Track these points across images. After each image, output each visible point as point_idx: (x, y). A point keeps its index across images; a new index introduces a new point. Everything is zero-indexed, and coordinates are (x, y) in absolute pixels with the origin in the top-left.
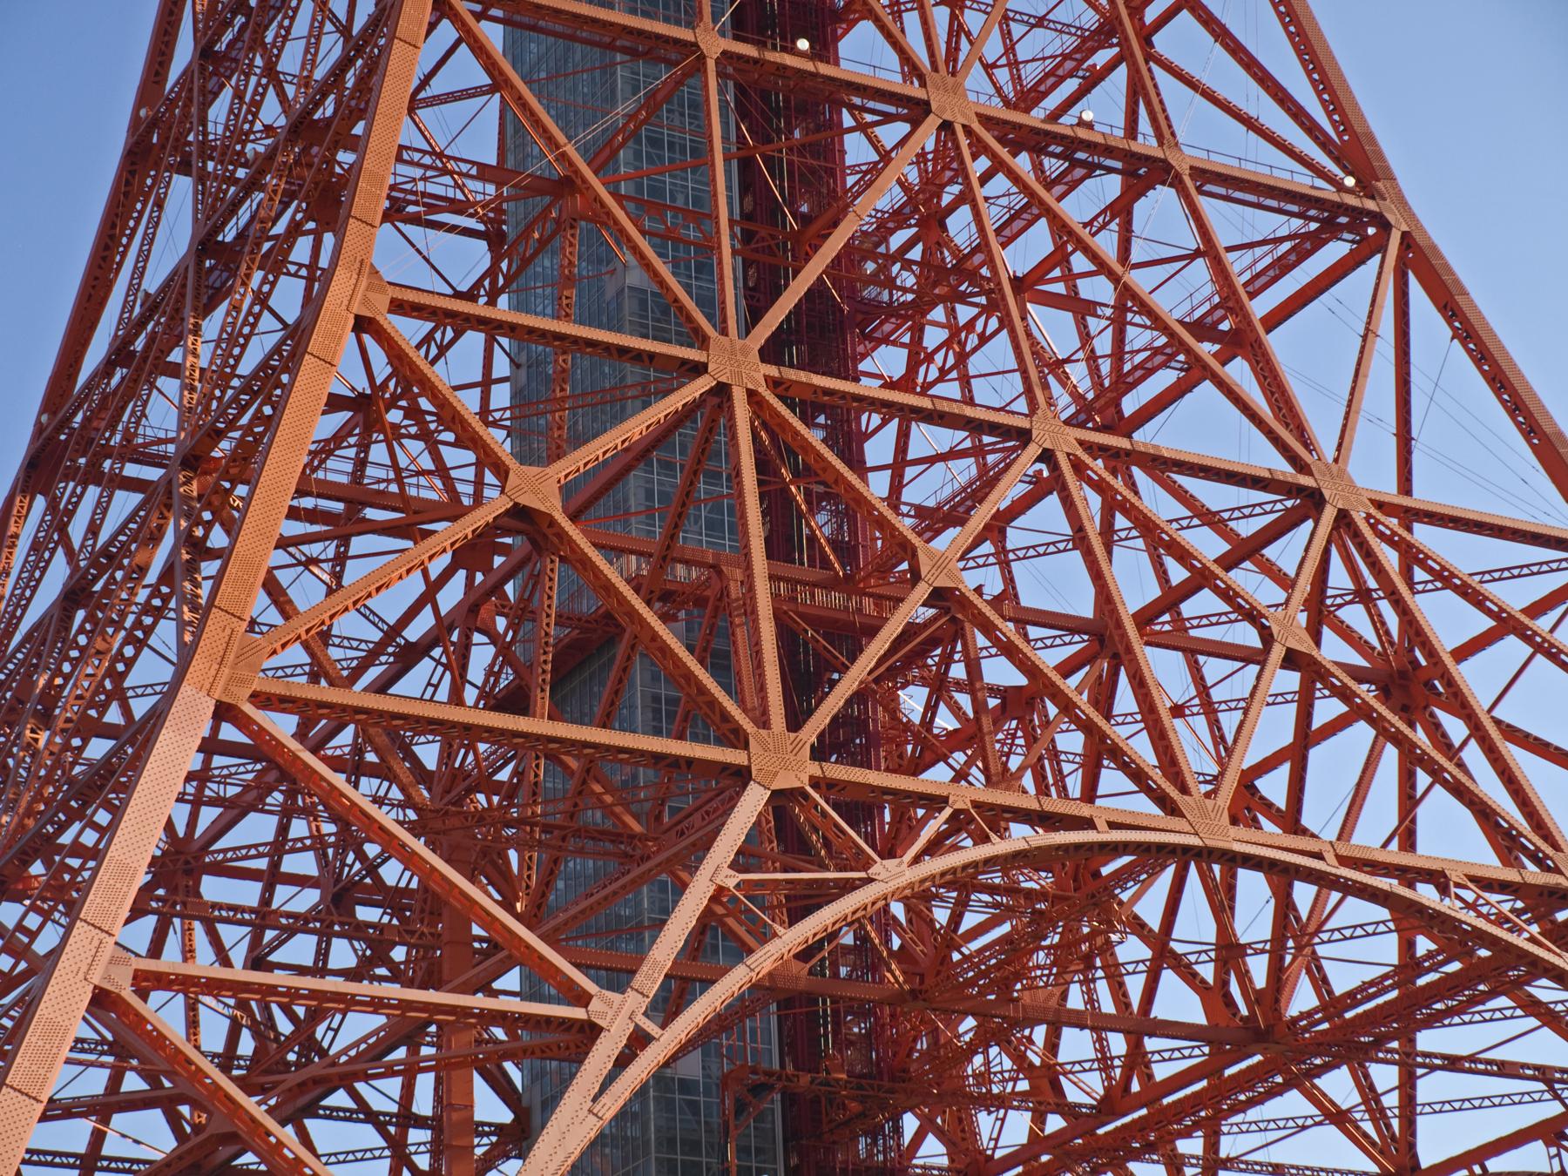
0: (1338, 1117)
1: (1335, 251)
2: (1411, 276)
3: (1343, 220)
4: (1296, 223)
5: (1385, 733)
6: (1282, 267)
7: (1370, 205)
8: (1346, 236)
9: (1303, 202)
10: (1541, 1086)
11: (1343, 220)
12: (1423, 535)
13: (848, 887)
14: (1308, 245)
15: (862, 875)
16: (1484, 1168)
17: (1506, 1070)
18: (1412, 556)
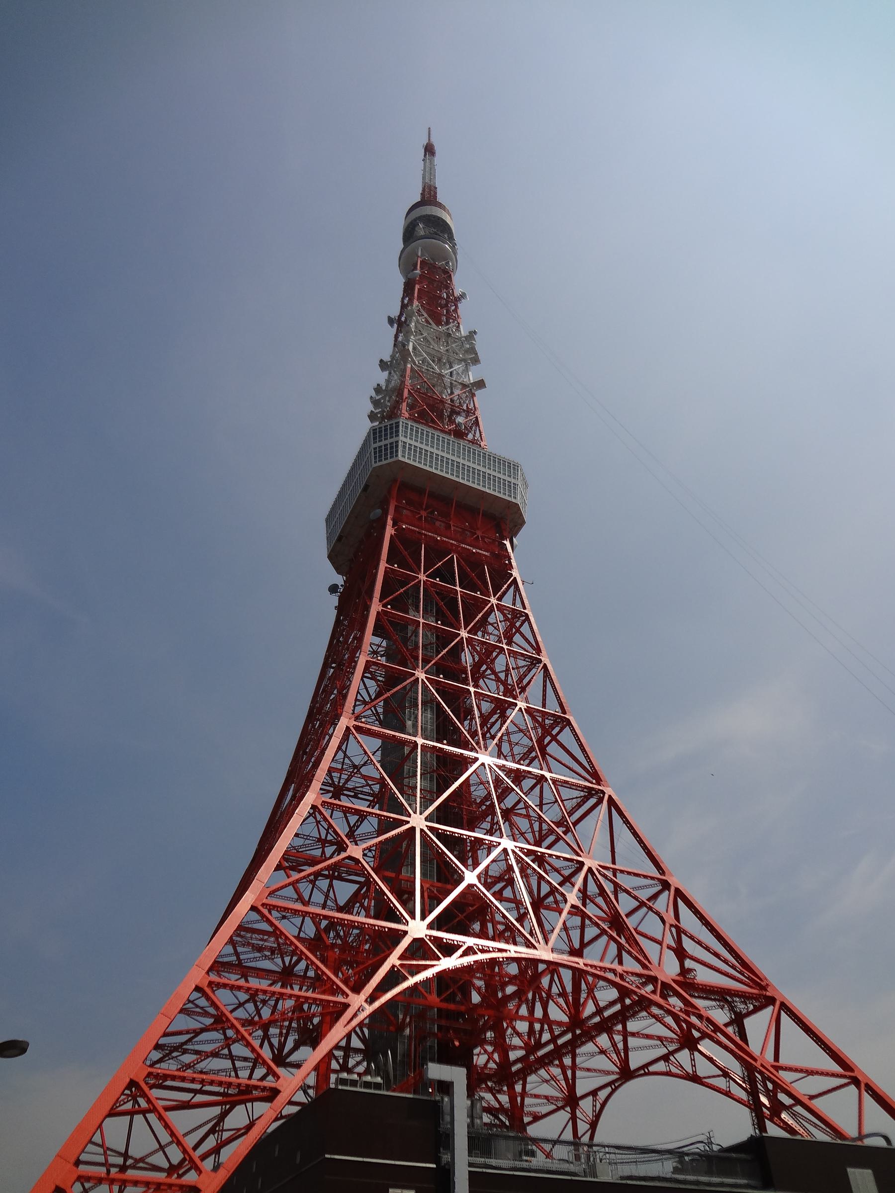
0: (602, 1052)
1: (593, 801)
3: (594, 792)
4: (582, 794)
5: (611, 938)
6: (579, 806)
8: (595, 797)
10: (659, 1042)
11: (594, 792)
12: (621, 879)
14: (585, 800)
16: (648, 1070)
17: (648, 1037)
18: (617, 886)
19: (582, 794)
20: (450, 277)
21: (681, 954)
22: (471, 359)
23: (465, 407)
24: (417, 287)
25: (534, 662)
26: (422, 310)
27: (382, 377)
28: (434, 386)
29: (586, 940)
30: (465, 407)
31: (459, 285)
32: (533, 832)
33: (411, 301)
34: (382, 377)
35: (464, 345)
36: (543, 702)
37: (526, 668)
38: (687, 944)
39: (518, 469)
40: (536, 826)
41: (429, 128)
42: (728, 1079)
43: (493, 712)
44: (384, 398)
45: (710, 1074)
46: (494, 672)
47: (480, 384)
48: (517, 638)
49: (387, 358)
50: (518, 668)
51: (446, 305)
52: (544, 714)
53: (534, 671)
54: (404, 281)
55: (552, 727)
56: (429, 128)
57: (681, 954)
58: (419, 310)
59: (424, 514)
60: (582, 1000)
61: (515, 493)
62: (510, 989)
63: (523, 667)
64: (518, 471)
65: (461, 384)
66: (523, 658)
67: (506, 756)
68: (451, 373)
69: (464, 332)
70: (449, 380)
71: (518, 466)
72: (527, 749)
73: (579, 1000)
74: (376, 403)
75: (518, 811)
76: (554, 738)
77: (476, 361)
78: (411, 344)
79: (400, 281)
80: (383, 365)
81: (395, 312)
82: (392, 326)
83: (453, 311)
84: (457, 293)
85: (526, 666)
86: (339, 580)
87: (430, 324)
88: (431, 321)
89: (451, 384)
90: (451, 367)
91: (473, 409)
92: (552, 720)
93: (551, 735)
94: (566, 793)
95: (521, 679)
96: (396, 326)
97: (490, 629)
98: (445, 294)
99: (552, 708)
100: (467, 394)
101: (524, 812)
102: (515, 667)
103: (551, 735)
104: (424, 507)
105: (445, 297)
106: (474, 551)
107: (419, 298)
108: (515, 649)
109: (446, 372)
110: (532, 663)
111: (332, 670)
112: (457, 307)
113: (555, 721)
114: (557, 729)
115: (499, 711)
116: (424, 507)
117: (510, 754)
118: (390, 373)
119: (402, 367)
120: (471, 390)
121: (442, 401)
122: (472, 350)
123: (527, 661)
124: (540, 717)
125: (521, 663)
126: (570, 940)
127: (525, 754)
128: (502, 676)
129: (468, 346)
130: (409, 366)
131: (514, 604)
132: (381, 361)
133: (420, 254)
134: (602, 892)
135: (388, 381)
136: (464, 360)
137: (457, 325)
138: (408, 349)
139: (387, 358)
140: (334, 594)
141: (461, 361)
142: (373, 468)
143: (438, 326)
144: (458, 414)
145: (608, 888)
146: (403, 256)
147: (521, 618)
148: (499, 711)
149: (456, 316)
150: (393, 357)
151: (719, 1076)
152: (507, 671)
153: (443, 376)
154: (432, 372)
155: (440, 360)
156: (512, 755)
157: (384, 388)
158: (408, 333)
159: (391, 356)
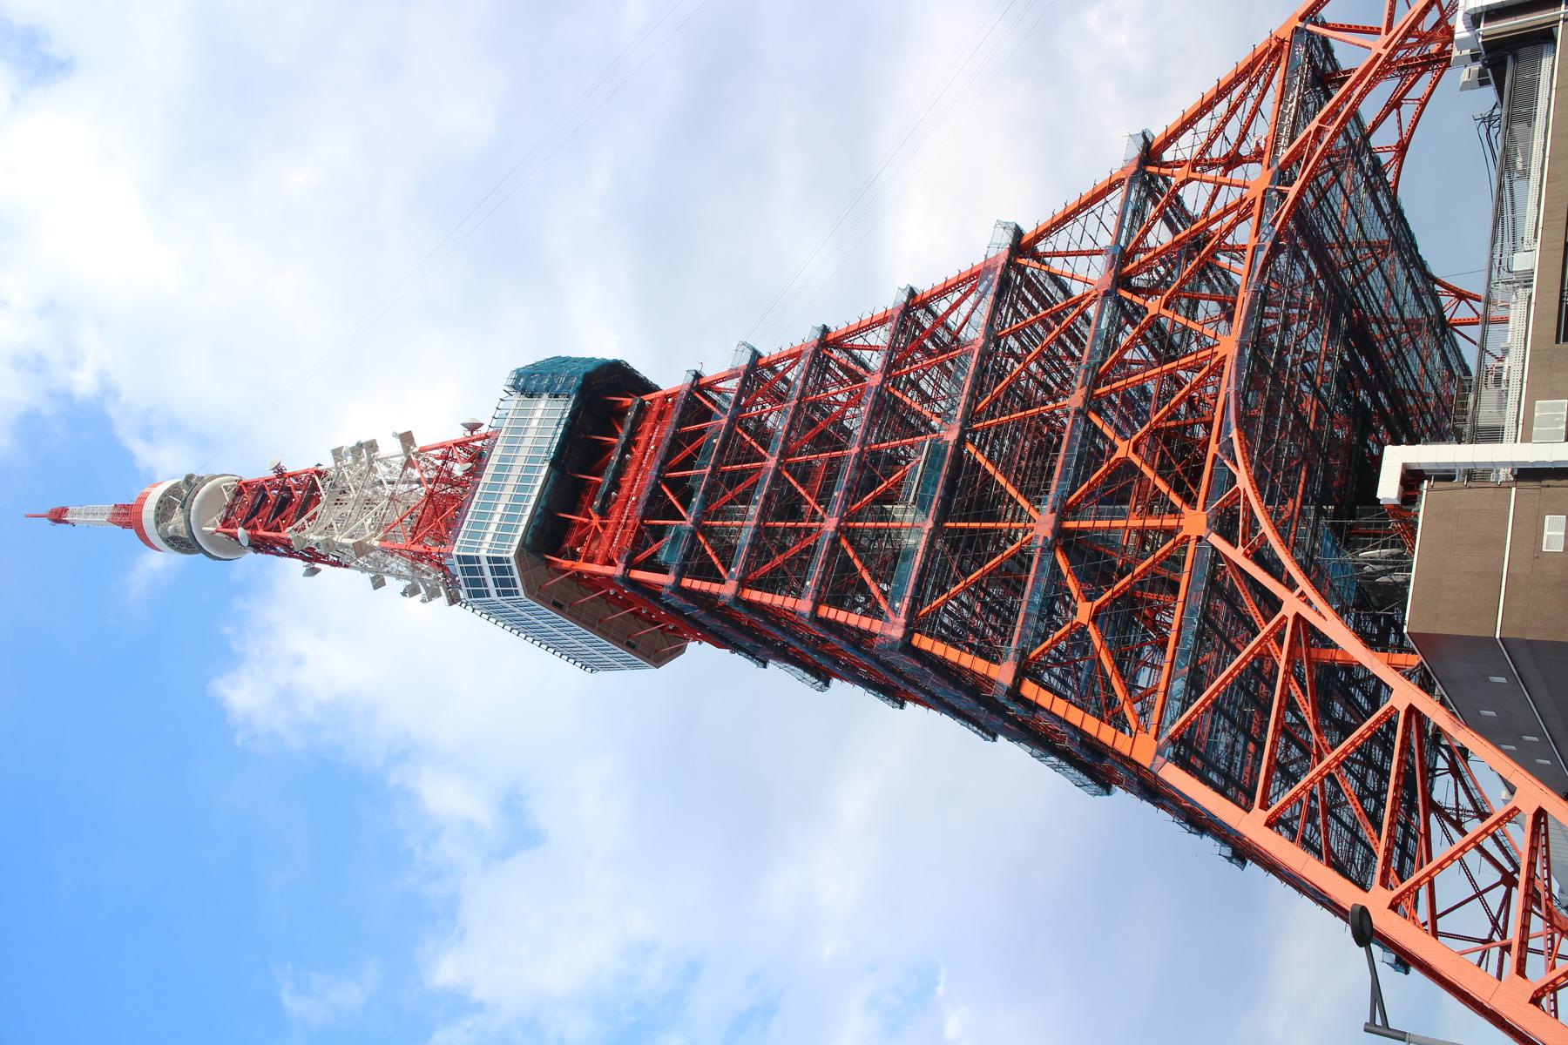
21: (1233, 160)
22: (369, 454)
23: (439, 463)
24: (261, 532)
26: (295, 526)
27: (394, 585)
28: (408, 508)
30: (439, 463)
31: (259, 470)
33: (278, 542)
34: (394, 585)
35: (348, 463)
38: (1218, 150)
41: (26, 516)
42: (1403, 101)
44: (423, 582)
45: (1397, 125)
47: (407, 439)
56: (26, 516)
57: (1233, 160)
58: (296, 530)
65: (405, 468)
68: (389, 483)
69: (328, 463)
74: (432, 594)
77: (372, 446)
80: (378, 583)
82: (317, 571)
84: (272, 474)
87: (316, 513)
88: (310, 513)
89: (404, 483)
90: (381, 483)
91: (442, 450)
96: (317, 565)
100: (420, 459)
104: (586, 520)
105: (276, 492)
106: (652, 447)
107: (277, 529)
112: (292, 475)
116: (586, 520)
118: (388, 572)
119: (379, 554)
120: (414, 454)
121: (430, 495)
129: (350, 458)
135: (399, 576)
136: (371, 461)
138: (353, 544)
141: (372, 469)
143: (319, 502)
144: (450, 473)
150: (364, 569)
151: (1399, 114)
153: (393, 493)
154: (387, 509)
157: (409, 583)
159: (362, 572)
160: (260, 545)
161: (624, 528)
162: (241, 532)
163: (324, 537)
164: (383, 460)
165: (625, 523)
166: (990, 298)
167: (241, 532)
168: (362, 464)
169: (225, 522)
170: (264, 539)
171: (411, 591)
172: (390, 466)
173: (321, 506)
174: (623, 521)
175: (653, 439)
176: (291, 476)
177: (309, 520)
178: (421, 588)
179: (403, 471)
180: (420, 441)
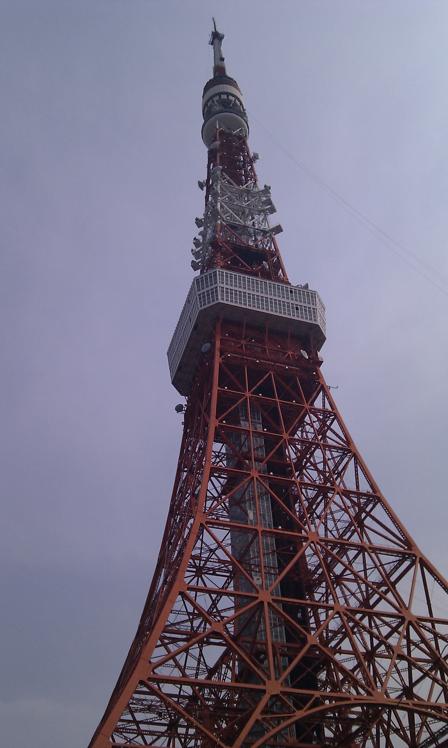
1: (407, 563)
2: (424, 569)
3: (407, 556)
4: (398, 558)
6: (396, 568)
7: (412, 552)
8: (408, 560)
9: (398, 553)
11: (407, 556)
13: (290, 717)
14: (401, 562)
15: (293, 715)
19: (398, 558)
20: (245, 143)
24: (218, 155)
25: (346, 452)
29: (414, 680)
32: (361, 592)
36: (356, 484)
37: (339, 458)
39: (315, 297)
40: (363, 587)
43: (317, 497)
46: (315, 465)
47: (278, 229)
48: (329, 433)
49: (201, 217)
50: (333, 458)
51: (244, 166)
52: (359, 495)
53: (346, 459)
54: (208, 150)
55: (366, 504)
59: (243, 342)
60: (416, 733)
61: (315, 317)
62: (355, 728)
63: (337, 457)
64: (315, 298)
65: (262, 231)
66: (336, 450)
67: (332, 531)
68: (253, 223)
70: (252, 229)
71: (315, 294)
72: (348, 524)
73: (415, 733)
74: (196, 254)
75: (345, 577)
76: (368, 514)
77: (273, 210)
78: (219, 204)
79: (204, 151)
81: (204, 178)
83: (250, 170)
85: (339, 456)
86: (183, 401)
87: (232, 184)
88: (232, 182)
89: (254, 232)
91: (274, 250)
92: (365, 499)
93: (366, 512)
94: (385, 558)
95: (337, 466)
96: (205, 188)
97: (308, 428)
98: (242, 157)
99: (365, 487)
100: (268, 238)
101: (352, 577)
102: (330, 457)
103: (366, 512)
105: (242, 160)
108: (330, 442)
109: (249, 223)
110: (344, 453)
111: (185, 474)
112: (252, 169)
113: (368, 500)
114: (371, 506)
115: (322, 494)
117: (335, 529)
122: (269, 202)
123: (340, 452)
124: (355, 497)
125: (335, 454)
126: (402, 680)
127: (346, 528)
128: (320, 467)
129: (265, 199)
130: (219, 222)
131: (324, 406)
132: (197, 219)
133: (218, 127)
134: (423, 640)
136: (263, 211)
137: (254, 181)
139: (201, 217)
140: (180, 412)
141: (260, 212)
142: (200, 311)
145: (428, 636)
146: (204, 129)
147: (331, 418)
148: (322, 494)
149: (253, 174)
150: (206, 215)
152: (325, 462)
155: (243, 213)
156: (336, 530)
158: (215, 196)
159: (204, 214)
160: (212, 156)
161: (241, 358)
162: (218, 143)
163: (219, 192)
164: (265, 219)
165: (244, 359)
166: (396, 548)
167: (218, 143)
168: (261, 206)
169: (222, 133)
170: (215, 158)
171: (197, 243)
172: (263, 222)
173: (237, 187)
174: (245, 357)
175: (292, 367)
176: (251, 167)
177: (228, 181)
178: (199, 248)
179: (260, 230)
180: (277, 237)
